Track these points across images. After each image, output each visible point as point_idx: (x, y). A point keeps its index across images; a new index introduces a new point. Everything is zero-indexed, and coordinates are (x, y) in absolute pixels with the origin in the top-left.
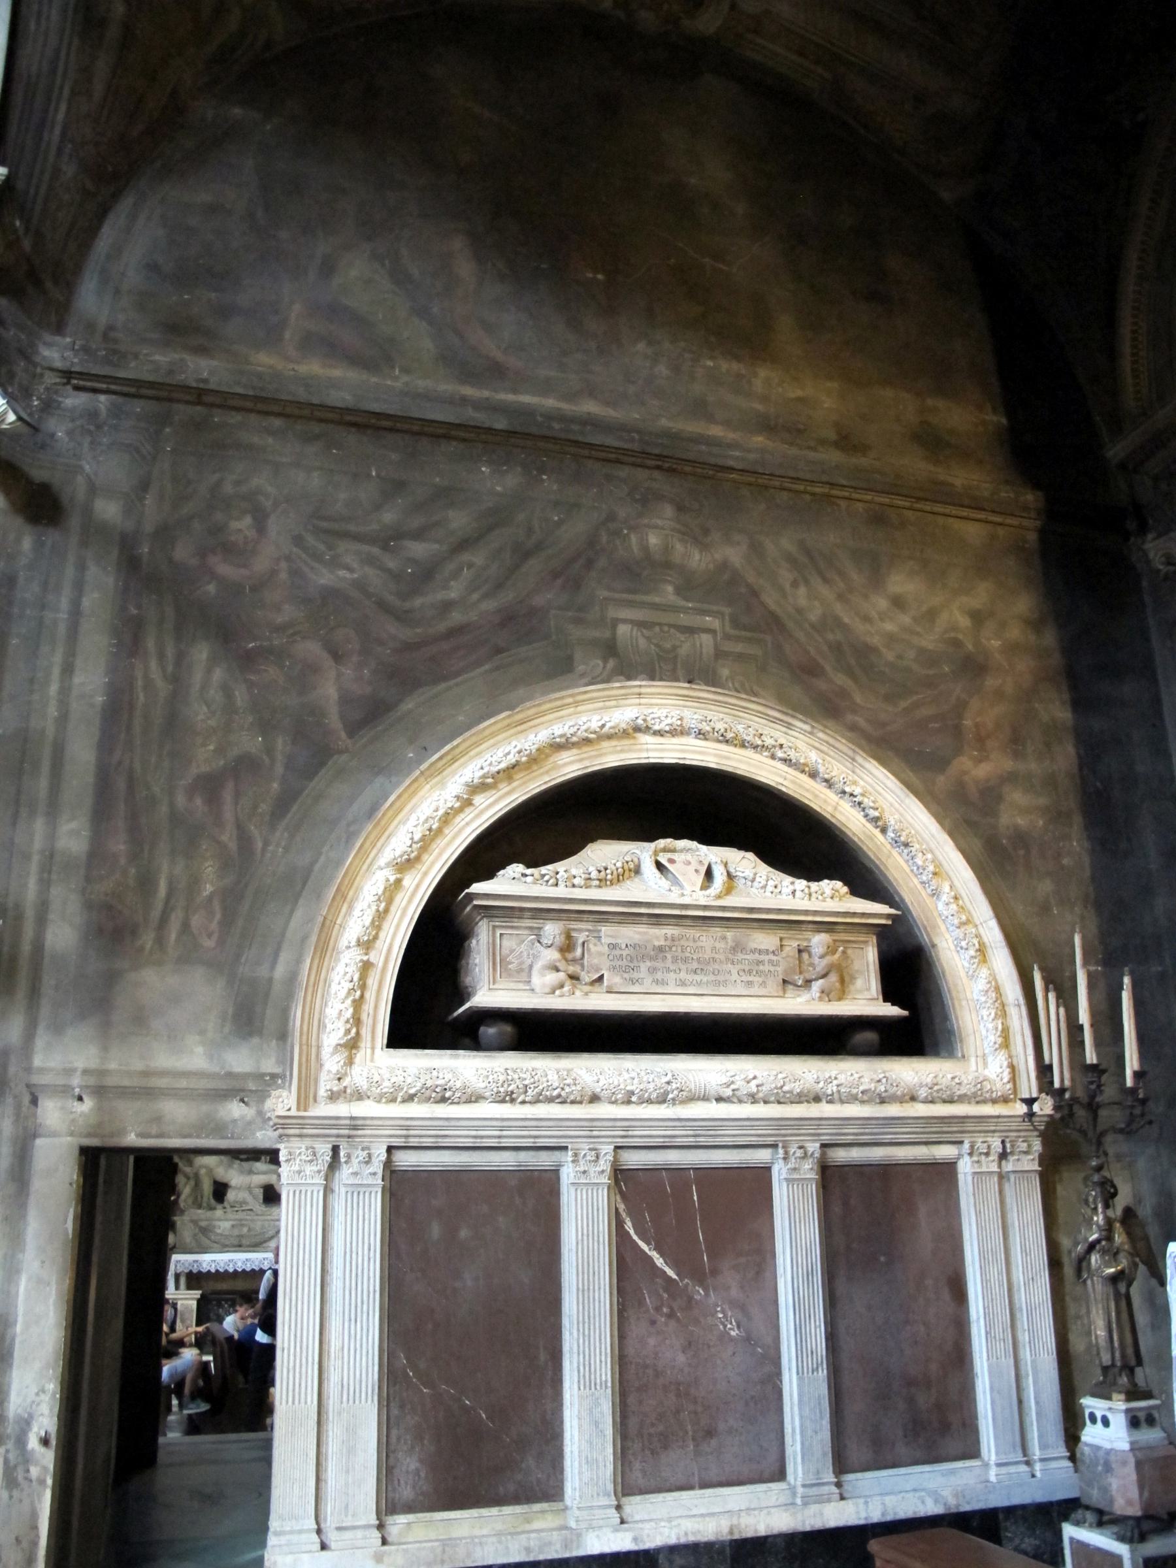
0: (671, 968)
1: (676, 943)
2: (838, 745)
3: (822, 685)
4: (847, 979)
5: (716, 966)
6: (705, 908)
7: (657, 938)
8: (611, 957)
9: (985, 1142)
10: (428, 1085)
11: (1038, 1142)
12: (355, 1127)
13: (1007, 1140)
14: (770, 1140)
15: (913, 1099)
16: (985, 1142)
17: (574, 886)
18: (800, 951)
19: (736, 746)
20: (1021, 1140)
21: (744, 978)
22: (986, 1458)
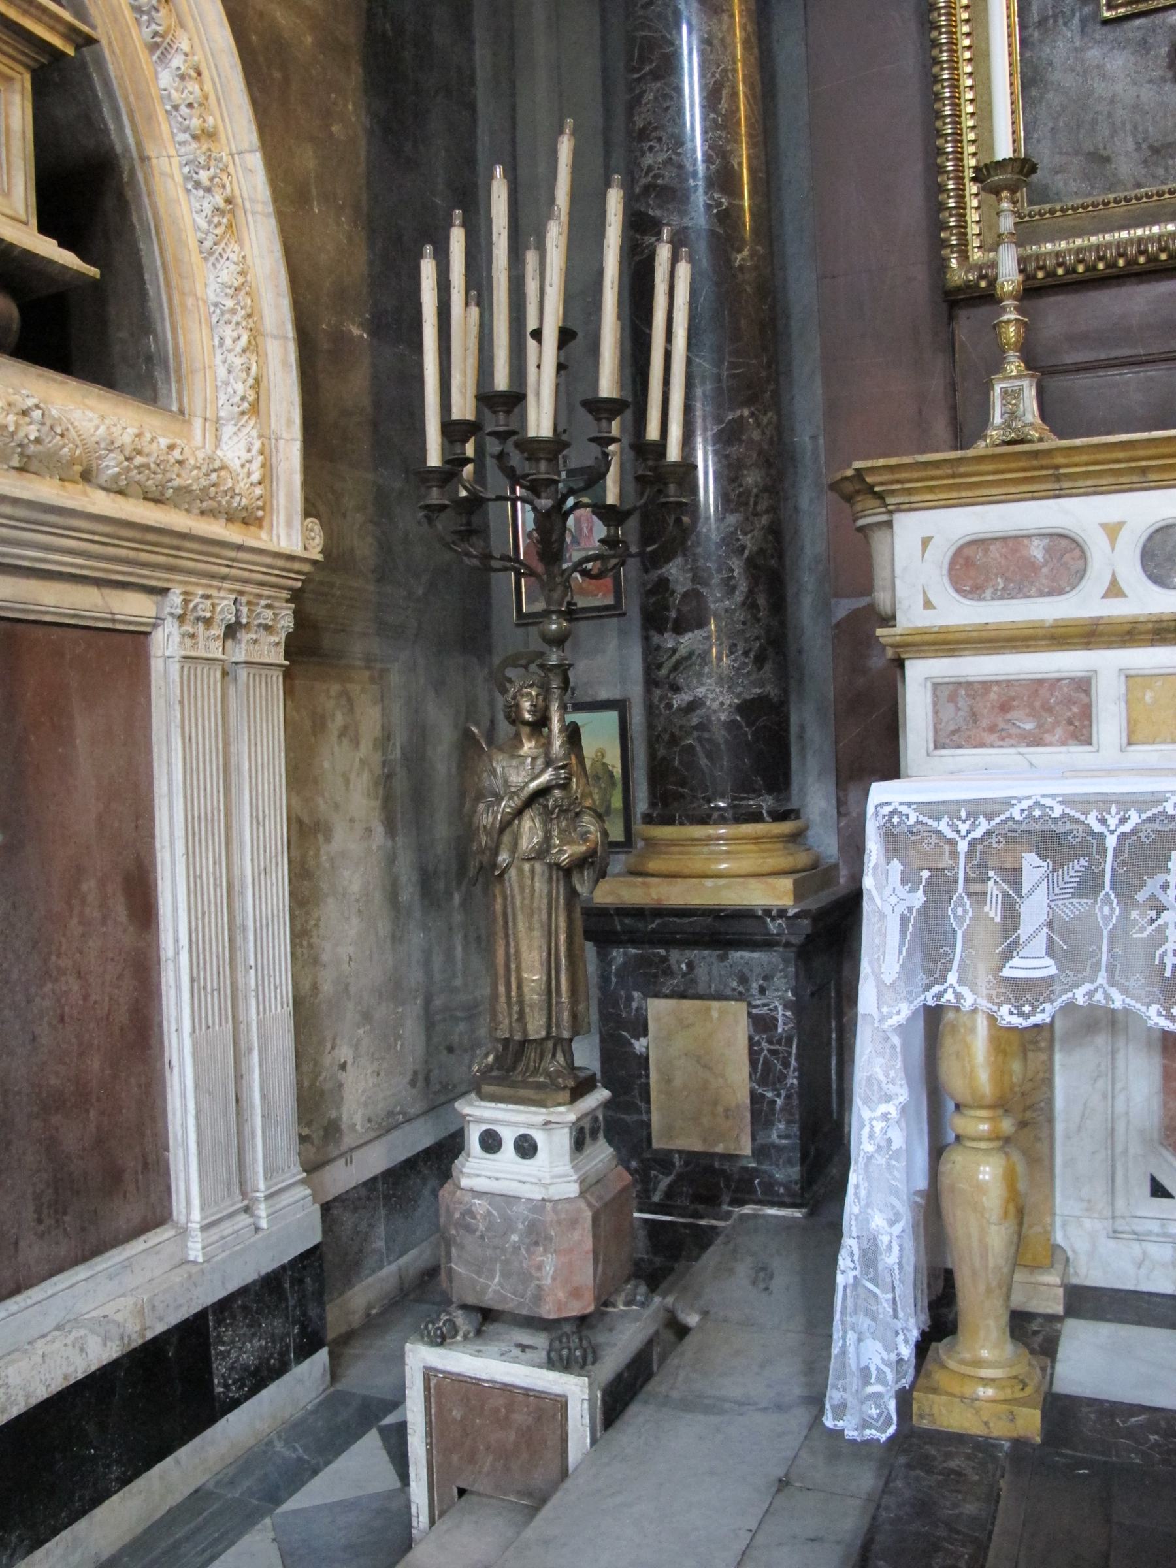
9: (208, 597)
11: (290, 612)
15: (86, 476)
16: (208, 597)
20: (263, 603)
22: (183, 1220)
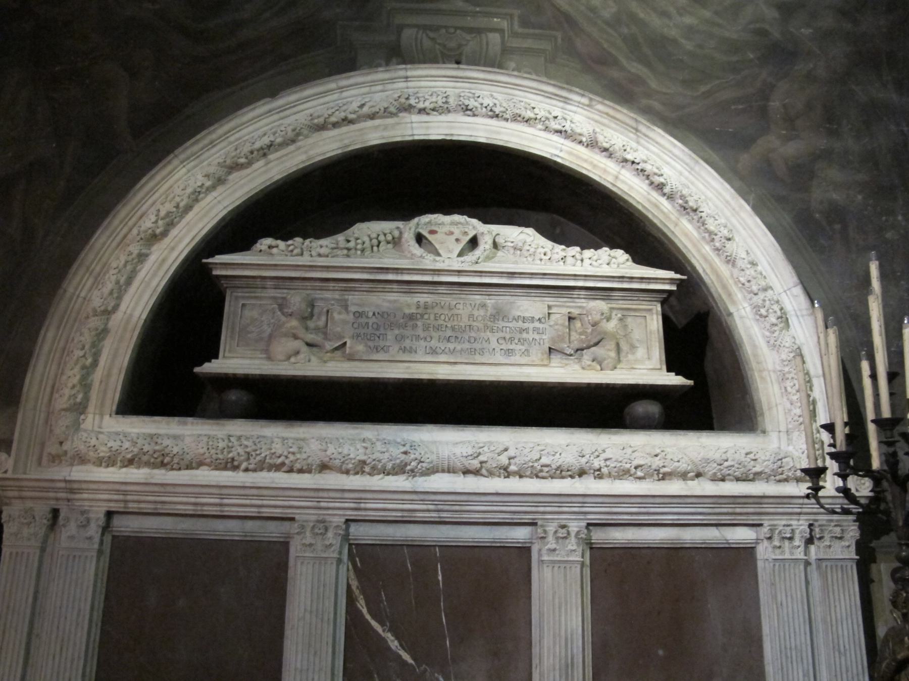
0: (422, 336)
1: (429, 311)
2: (618, 116)
3: (615, 74)
4: (624, 347)
5: (473, 334)
6: (459, 272)
7: (409, 306)
8: (356, 325)
10: (145, 450)
11: (856, 528)
12: (72, 491)
13: (816, 524)
14: (527, 518)
17: (320, 255)
18: (570, 319)
19: (507, 120)
20: (833, 524)
21: (504, 347)
